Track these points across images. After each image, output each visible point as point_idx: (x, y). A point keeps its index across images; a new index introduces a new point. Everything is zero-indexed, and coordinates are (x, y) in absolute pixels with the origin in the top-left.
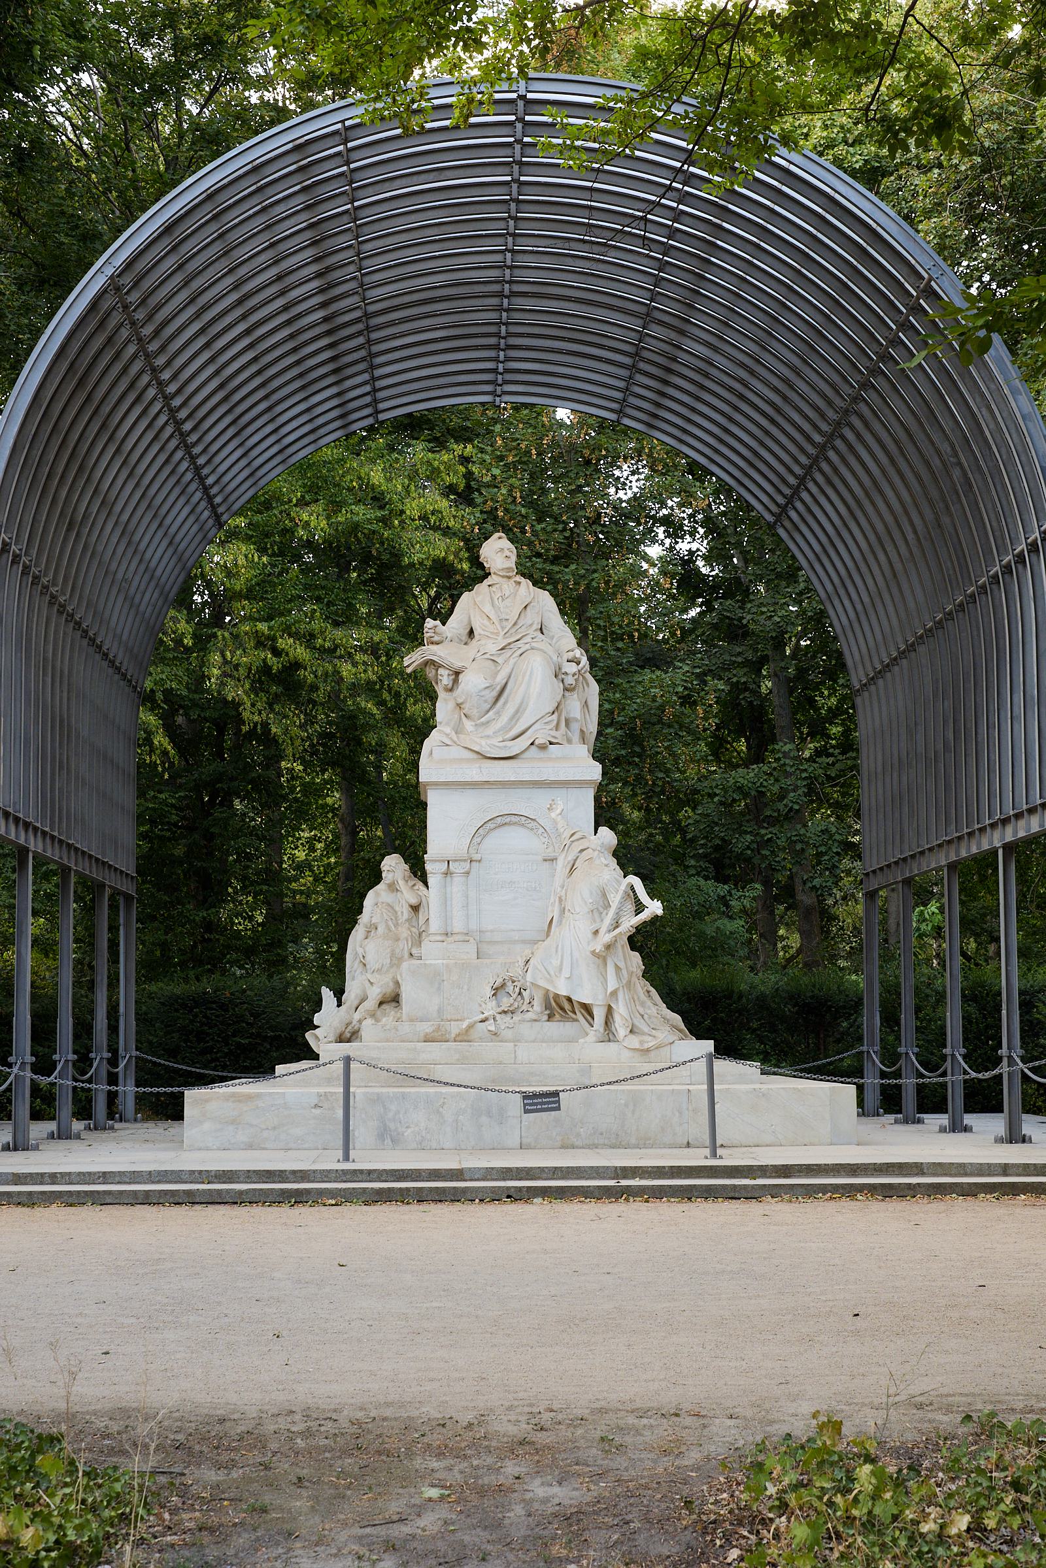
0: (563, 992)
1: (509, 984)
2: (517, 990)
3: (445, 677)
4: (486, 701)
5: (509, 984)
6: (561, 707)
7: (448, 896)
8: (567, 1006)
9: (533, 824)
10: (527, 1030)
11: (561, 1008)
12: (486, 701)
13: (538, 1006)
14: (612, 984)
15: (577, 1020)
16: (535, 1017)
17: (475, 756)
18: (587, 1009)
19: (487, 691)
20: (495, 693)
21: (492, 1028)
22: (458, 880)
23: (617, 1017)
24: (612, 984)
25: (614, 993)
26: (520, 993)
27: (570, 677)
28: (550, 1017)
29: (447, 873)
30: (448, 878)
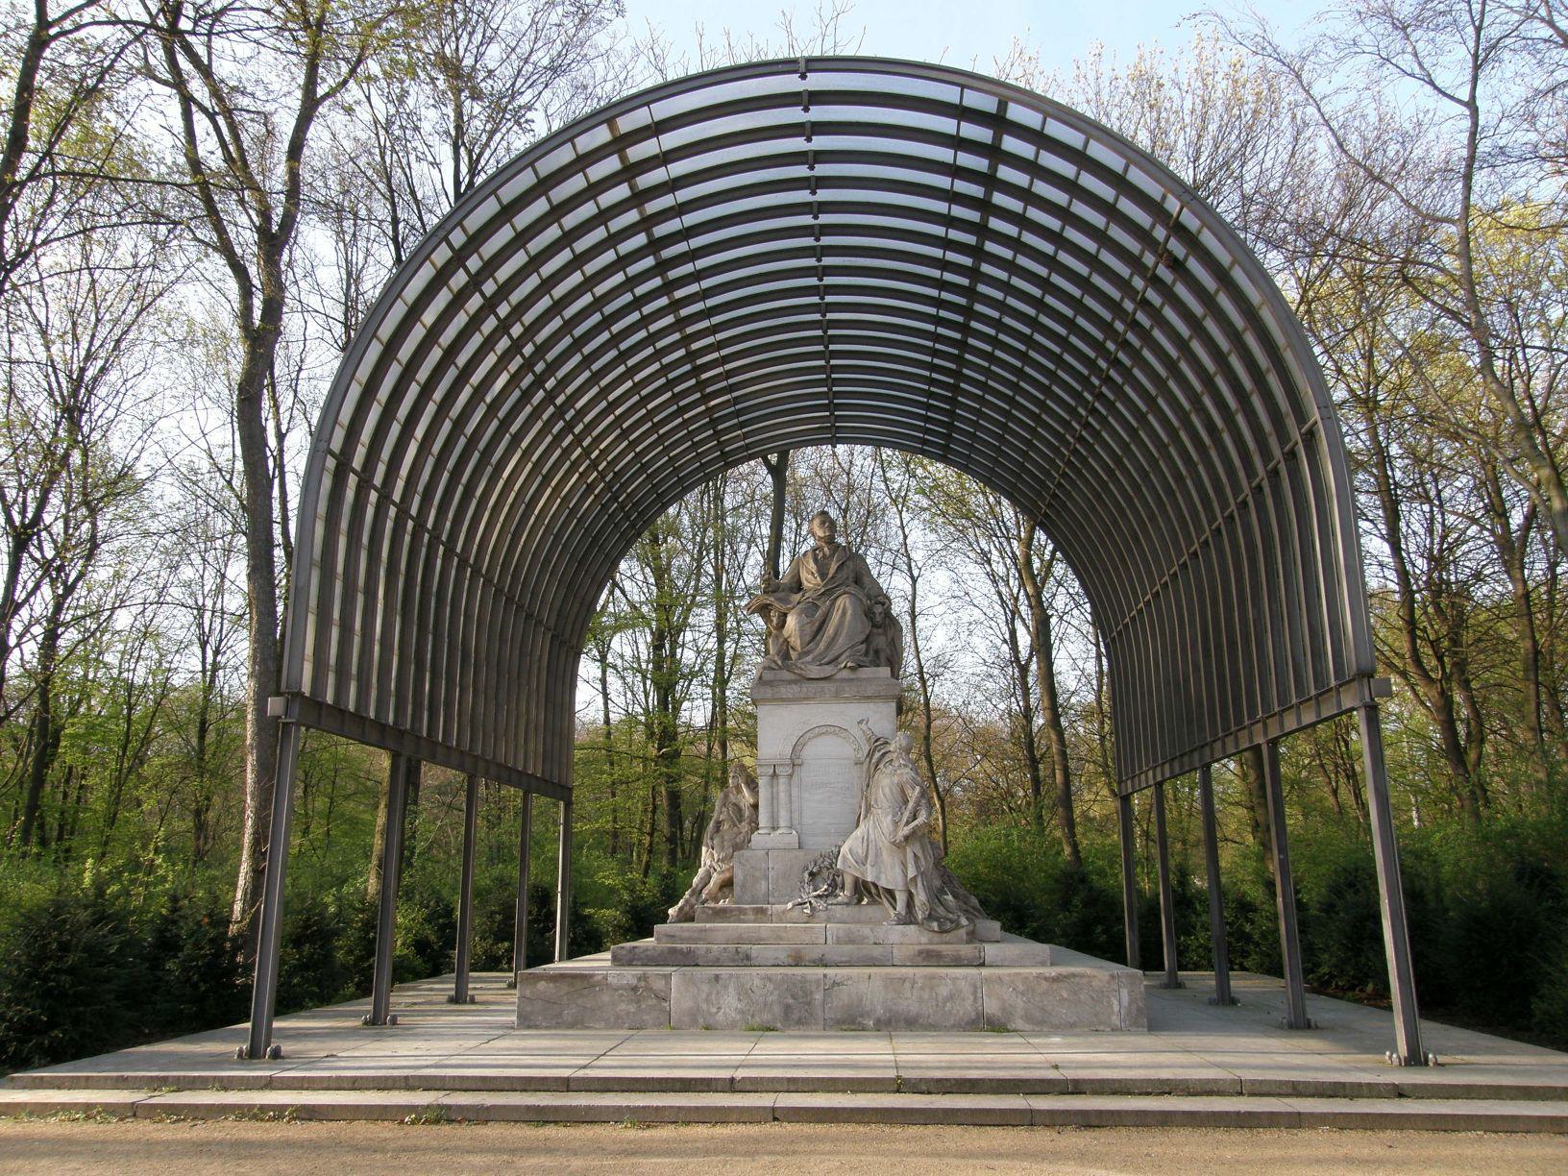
10: (839, 911)
18: (890, 893)
23: (917, 902)
29: (774, 775)
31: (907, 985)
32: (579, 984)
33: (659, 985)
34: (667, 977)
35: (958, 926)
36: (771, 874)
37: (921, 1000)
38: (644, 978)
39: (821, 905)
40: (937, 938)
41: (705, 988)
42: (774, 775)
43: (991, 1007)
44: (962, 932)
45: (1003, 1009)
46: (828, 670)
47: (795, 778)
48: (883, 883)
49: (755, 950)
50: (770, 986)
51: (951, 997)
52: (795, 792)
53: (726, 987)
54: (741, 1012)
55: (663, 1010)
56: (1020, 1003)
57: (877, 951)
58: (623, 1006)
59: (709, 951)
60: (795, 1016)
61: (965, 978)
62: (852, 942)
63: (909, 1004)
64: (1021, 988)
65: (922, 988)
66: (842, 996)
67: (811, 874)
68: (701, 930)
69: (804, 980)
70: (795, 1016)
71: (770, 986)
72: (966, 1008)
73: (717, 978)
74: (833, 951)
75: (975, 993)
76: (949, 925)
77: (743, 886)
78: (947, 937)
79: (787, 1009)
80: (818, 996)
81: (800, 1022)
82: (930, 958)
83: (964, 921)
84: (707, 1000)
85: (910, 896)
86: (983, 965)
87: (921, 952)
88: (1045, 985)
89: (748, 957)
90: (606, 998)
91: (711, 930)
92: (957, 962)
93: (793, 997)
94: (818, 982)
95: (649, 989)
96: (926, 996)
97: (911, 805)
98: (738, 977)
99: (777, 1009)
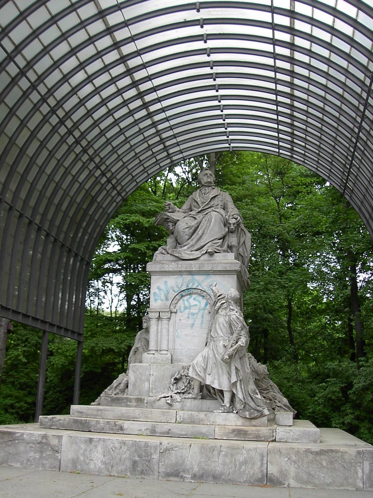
0: (208, 383)
1: (184, 377)
2: (188, 381)
3: (171, 226)
4: (186, 235)
5: (184, 377)
6: (227, 238)
7: (159, 331)
8: (212, 391)
9: (205, 294)
10: (189, 403)
11: (208, 393)
12: (186, 235)
13: (196, 390)
14: (234, 379)
15: (217, 399)
16: (194, 396)
17: (178, 259)
19: (187, 229)
20: (191, 231)
21: (169, 402)
22: (165, 322)
24: (234, 379)
25: (235, 384)
26: (189, 383)
27: (232, 225)
28: (203, 398)
29: (159, 318)
30: (160, 322)
31: (216, 453)
32: (6, 438)
33: (54, 442)
34: (60, 437)
35: (262, 415)
36: (152, 378)
37: (224, 464)
38: (45, 437)
39: (178, 397)
40: (248, 423)
41: (83, 446)
42: (159, 318)
43: (273, 470)
44: (265, 418)
45: (281, 472)
46: (197, 254)
47: (172, 321)
48: (216, 386)
49: (126, 425)
50: (125, 449)
51: (245, 462)
52: (171, 329)
53: (96, 446)
54: (104, 463)
55: (56, 459)
56: (292, 470)
57: (204, 429)
58: (32, 454)
59: (98, 422)
60: (139, 469)
61: (256, 449)
62: (193, 422)
63: (218, 465)
64: (294, 458)
65: (225, 456)
66: (172, 458)
67: (176, 379)
68: (98, 410)
69: (147, 445)
70: (139, 469)
71: (125, 449)
72: (255, 470)
73: (91, 440)
74: (177, 428)
75: (262, 460)
76: (256, 414)
77: (134, 385)
78: (254, 422)
79: (135, 463)
80: (155, 457)
81: (142, 472)
82: (240, 434)
83: (266, 412)
84: (83, 454)
85: (233, 396)
86: (274, 441)
87: (234, 431)
88: (311, 456)
89: (121, 428)
90: (22, 448)
91: (105, 410)
92: (258, 439)
93: (140, 456)
94: (155, 447)
95: (48, 444)
96: (228, 461)
97: (235, 335)
98: (104, 440)
99: (128, 464)
